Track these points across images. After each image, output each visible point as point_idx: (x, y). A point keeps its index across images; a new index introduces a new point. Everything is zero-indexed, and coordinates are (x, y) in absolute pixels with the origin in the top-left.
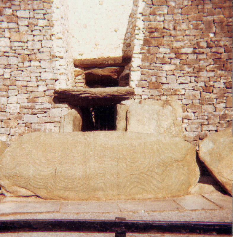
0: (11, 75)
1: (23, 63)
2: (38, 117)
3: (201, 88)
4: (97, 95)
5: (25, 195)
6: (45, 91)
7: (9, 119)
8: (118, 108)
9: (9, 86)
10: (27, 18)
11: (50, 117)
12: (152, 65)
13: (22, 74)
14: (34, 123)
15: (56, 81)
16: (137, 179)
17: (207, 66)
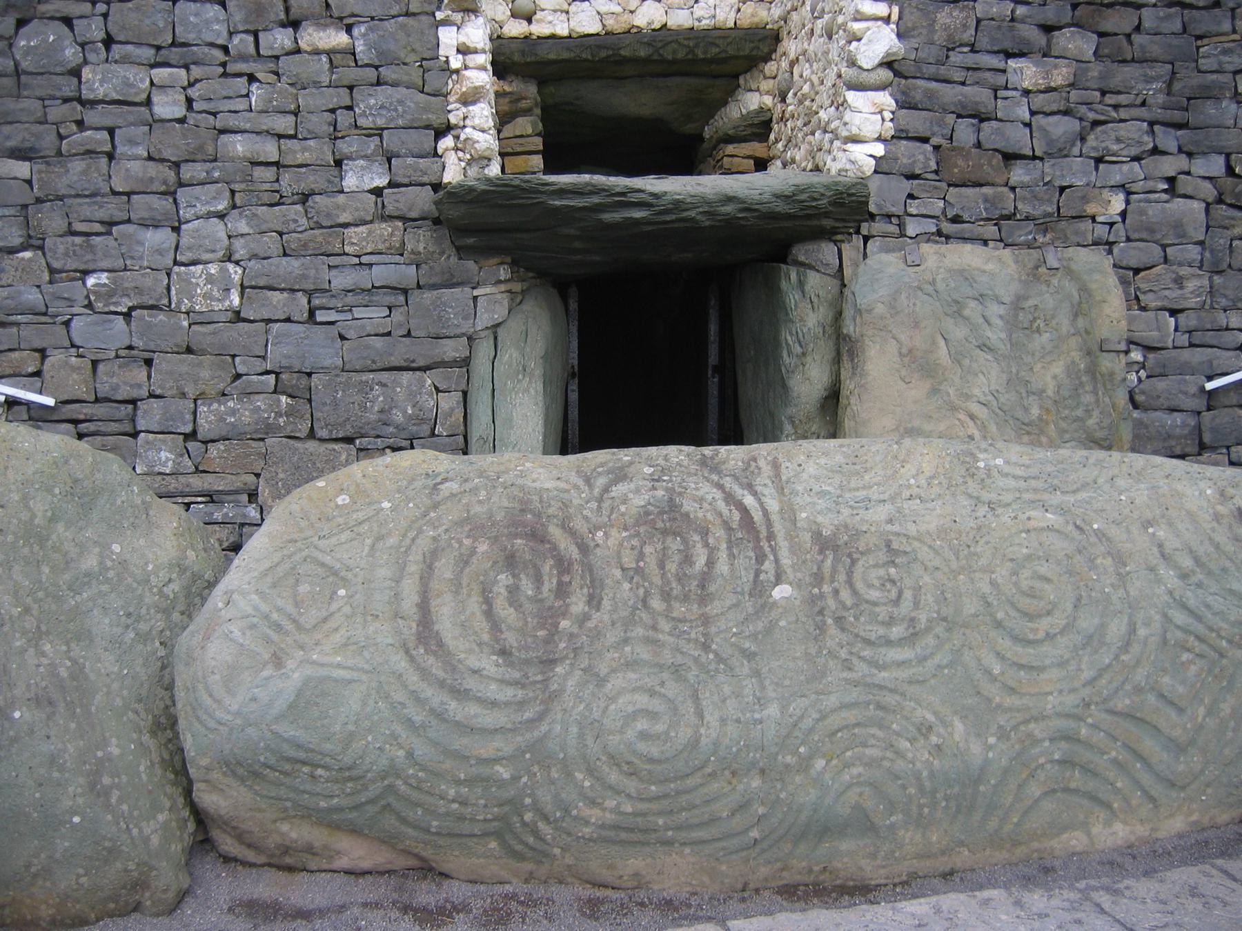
0: (189, 101)
2: (342, 338)
3: (1208, 185)
4: (692, 214)
5: (366, 865)
6: (377, 192)
7: (189, 350)
8: (784, 285)
9: (177, 165)
11: (409, 334)
12: (955, 58)
13: (247, 95)
14: (325, 370)
15: (440, 133)
16: (1063, 744)
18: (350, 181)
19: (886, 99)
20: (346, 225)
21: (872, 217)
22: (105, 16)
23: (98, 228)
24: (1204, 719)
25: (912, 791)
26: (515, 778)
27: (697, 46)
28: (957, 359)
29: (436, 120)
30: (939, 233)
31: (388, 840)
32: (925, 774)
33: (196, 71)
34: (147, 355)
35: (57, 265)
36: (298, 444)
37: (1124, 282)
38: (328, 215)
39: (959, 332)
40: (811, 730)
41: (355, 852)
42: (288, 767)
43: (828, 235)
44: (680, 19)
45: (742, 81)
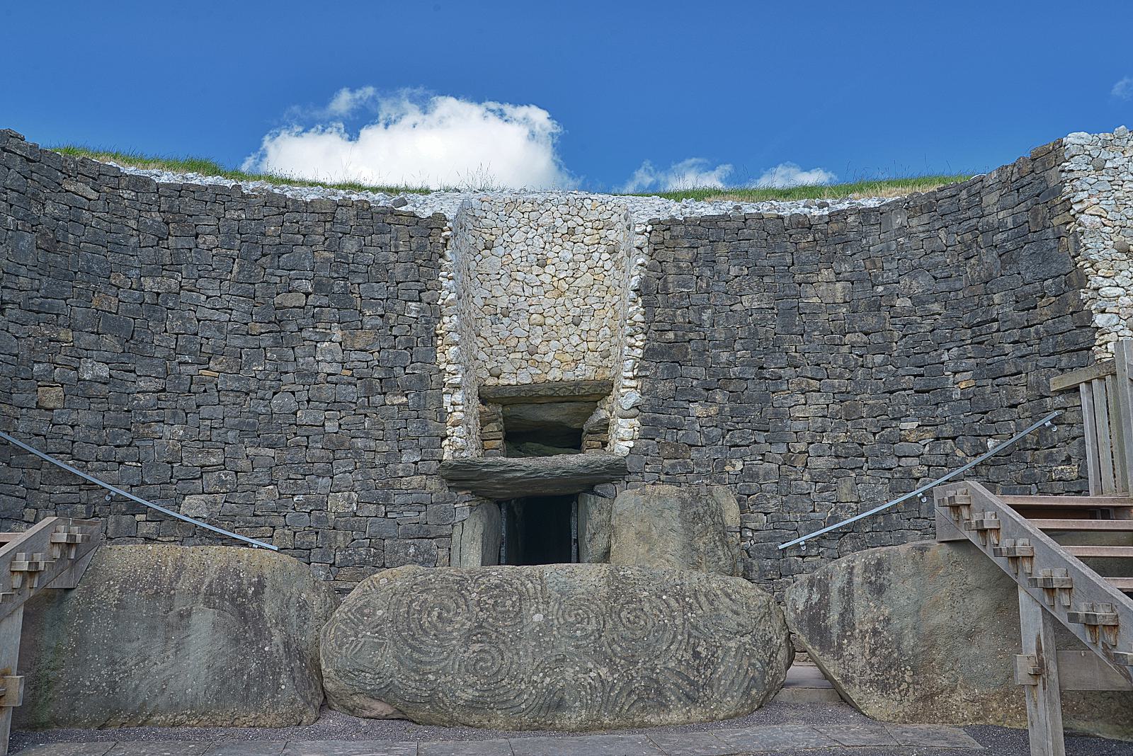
0: (340, 425)
1: (368, 397)
2: (398, 524)
4: (542, 474)
6: (416, 463)
7: (334, 528)
9: (334, 451)
10: (382, 300)
15: (443, 439)
17: (789, 408)
18: (404, 459)
19: (636, 422)
20: (402, 477)
21: (630, 473)
22: (308, 390)
23: (300, 477)
24: (711, 674)
25: (583, 693)
26: (436, 680)
27: (574, 389)
28: (660, 536)
29: (442, 435)
30: (660, 480)
31: (390, 704)
32: (588, 687)
33: (343, 413)
34: (317, 530)
35: (281, 491)
36: (377, 570)
37: (739, 500)
38: (395, 472)
39: (662, 524)
40: (545, 668)
41: (380, 708)
42: (356, 673)
43: (610, 481)
44: (569, 376)
45: (598, 404)
